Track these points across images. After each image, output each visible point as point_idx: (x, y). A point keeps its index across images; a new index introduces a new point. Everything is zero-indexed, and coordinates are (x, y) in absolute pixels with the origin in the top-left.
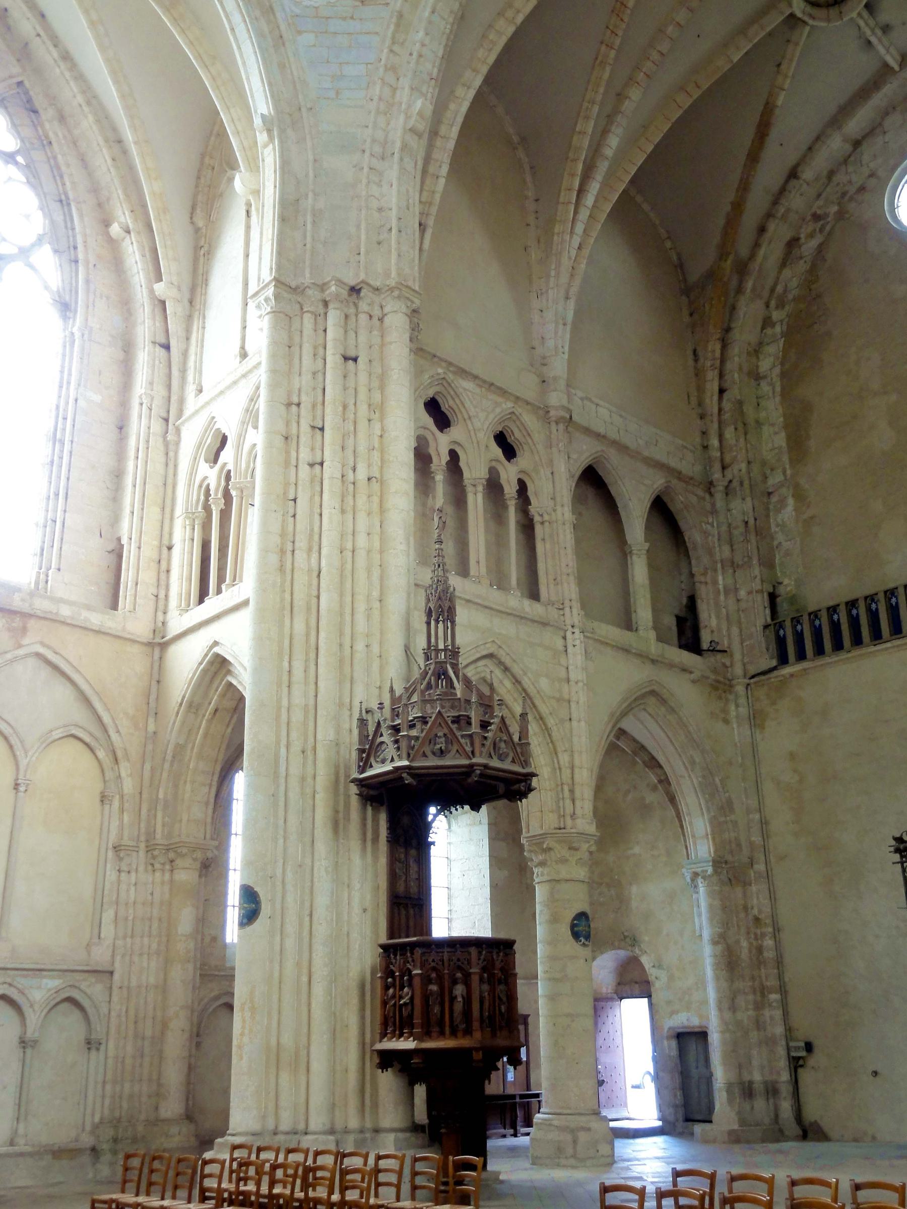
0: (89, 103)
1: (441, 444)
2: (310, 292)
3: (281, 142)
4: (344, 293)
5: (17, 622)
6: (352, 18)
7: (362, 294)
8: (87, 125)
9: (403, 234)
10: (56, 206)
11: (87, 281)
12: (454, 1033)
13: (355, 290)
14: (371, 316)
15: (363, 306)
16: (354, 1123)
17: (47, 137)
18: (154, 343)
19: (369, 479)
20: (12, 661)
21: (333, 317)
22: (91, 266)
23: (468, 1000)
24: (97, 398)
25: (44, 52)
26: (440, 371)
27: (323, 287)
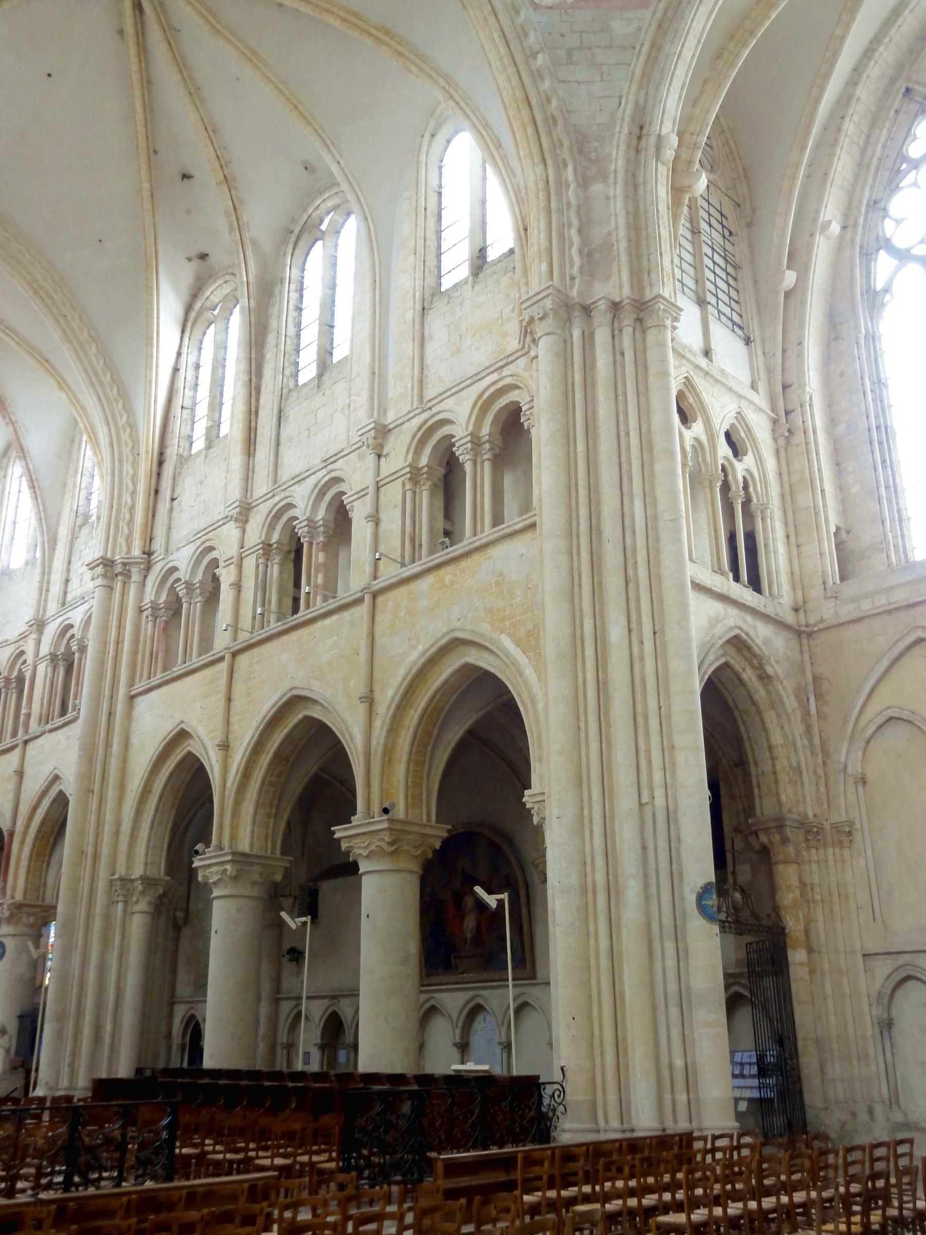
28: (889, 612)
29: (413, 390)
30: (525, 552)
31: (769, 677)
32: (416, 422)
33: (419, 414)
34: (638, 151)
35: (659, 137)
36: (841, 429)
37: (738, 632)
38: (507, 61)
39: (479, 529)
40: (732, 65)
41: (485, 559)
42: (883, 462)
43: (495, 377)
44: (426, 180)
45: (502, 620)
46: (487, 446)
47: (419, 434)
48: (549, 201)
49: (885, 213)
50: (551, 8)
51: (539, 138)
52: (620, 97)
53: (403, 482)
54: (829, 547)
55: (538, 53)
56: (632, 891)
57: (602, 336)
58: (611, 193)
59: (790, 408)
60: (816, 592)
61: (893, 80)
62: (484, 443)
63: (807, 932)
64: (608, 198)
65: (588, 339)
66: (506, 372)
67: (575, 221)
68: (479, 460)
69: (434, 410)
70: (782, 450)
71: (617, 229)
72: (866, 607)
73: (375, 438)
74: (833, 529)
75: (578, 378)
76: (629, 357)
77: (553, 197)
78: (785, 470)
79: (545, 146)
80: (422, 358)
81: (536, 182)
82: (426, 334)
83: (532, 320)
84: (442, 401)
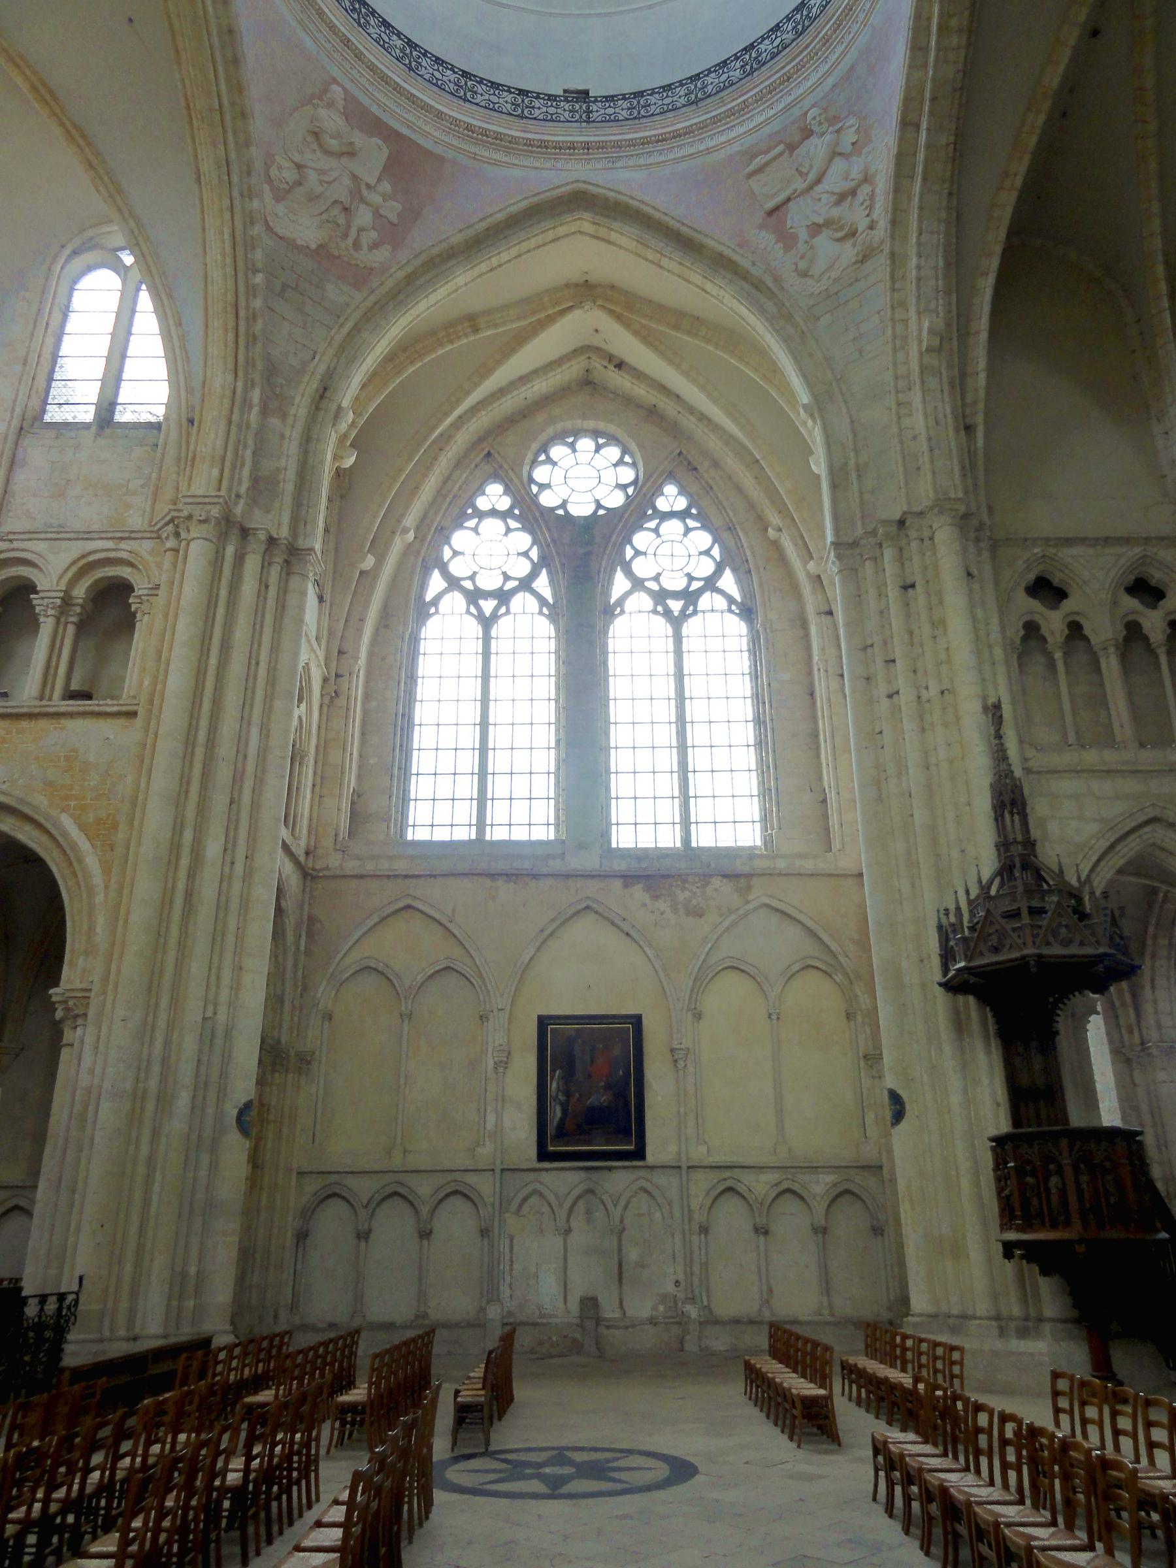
0: (727, 444)
1: (1054, 622)
2: (863, 542)
3: (823, 419)
4: (893, 529)
5: (742, 882)
6: (857, 280)
7: (907, 524)
8: (731, 462)
9: (937, 452)
10: (726, 535)
11: (761, 584)
12: (1054, 1226)
13: (901, 523)
14: (922, 540)
15: (913, 534)
16: (1017, 1311)
17: (707, 483)
18: (819, 614)
19: (942, 693)
20: (746, 915)
21: (888, 554)
22: (762, 570)
23: (1063, 1192)
24: (787, 677)
25: (688, 423)
26: (1036, 550)
27: (874, 533)
28: (389, 877)
30: (112, 737)
34: (317, 408)
35: (339, 407)
36: (373, 704)
38: (229, 260)
40: (399, 373)
41: (55, 728)
43: (109, 544)
45: (68, 798)
46: (78, 609)
49: (447, 541)
50: (281, 238)
51: (237, 348)
52: (315, 352)
54: (345, 805)
55: (258, 271)
56: (183, 1102)
57: (252, 563)
58: (287, 434)
59: (340, 672)
60: (327, 843)
61: (481, 440)
64: (282, 436)
65: (240, 559)
66: (123, 545)
67: (250, 442)
68: (63, 619)
69: (16, 544)
70: (325, 708)
72: (370, 867)
75: (224, 593)
76: (272, 592)
78: (323, 726)
79: (241, 358)
81: (223, 387)
82: (19, 456)
83: (190, 517)
84: (30, 540)
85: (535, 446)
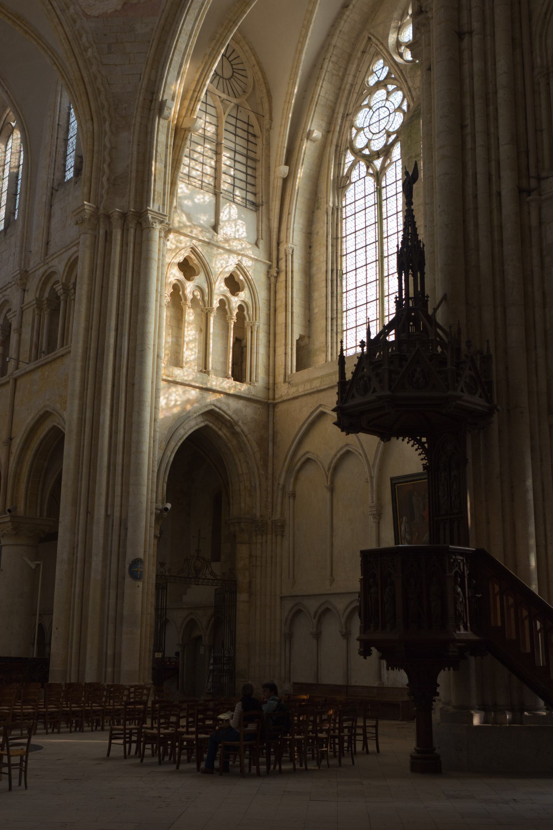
29: (42, 249)
31: (237, 433)
32: (41, 271)
33: (43, 266)
37: (213, 407)
39: (65, 343)
42: (332, 293)
44: (60, 103)
47: (43, 279)
48: (93, 145)
50: (98, 17)
51: (89, 103)
53: (34, 309)
55: (88, 48)
62: (71, 290)
63: (250, 583)
65: (108, 237)
67: (108, 159)
71: (131, 163)
73: (21, 279)
74: (296, 337)
77: (96, 143)
79: (93, 109)
80: (49, 228)
85: (396, 15)
